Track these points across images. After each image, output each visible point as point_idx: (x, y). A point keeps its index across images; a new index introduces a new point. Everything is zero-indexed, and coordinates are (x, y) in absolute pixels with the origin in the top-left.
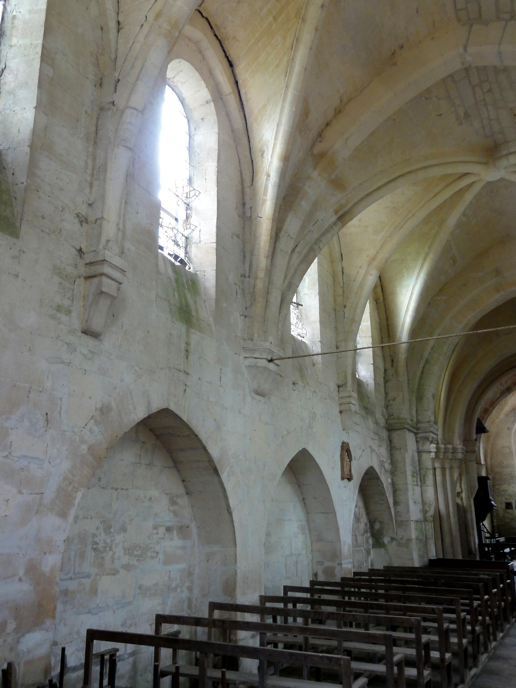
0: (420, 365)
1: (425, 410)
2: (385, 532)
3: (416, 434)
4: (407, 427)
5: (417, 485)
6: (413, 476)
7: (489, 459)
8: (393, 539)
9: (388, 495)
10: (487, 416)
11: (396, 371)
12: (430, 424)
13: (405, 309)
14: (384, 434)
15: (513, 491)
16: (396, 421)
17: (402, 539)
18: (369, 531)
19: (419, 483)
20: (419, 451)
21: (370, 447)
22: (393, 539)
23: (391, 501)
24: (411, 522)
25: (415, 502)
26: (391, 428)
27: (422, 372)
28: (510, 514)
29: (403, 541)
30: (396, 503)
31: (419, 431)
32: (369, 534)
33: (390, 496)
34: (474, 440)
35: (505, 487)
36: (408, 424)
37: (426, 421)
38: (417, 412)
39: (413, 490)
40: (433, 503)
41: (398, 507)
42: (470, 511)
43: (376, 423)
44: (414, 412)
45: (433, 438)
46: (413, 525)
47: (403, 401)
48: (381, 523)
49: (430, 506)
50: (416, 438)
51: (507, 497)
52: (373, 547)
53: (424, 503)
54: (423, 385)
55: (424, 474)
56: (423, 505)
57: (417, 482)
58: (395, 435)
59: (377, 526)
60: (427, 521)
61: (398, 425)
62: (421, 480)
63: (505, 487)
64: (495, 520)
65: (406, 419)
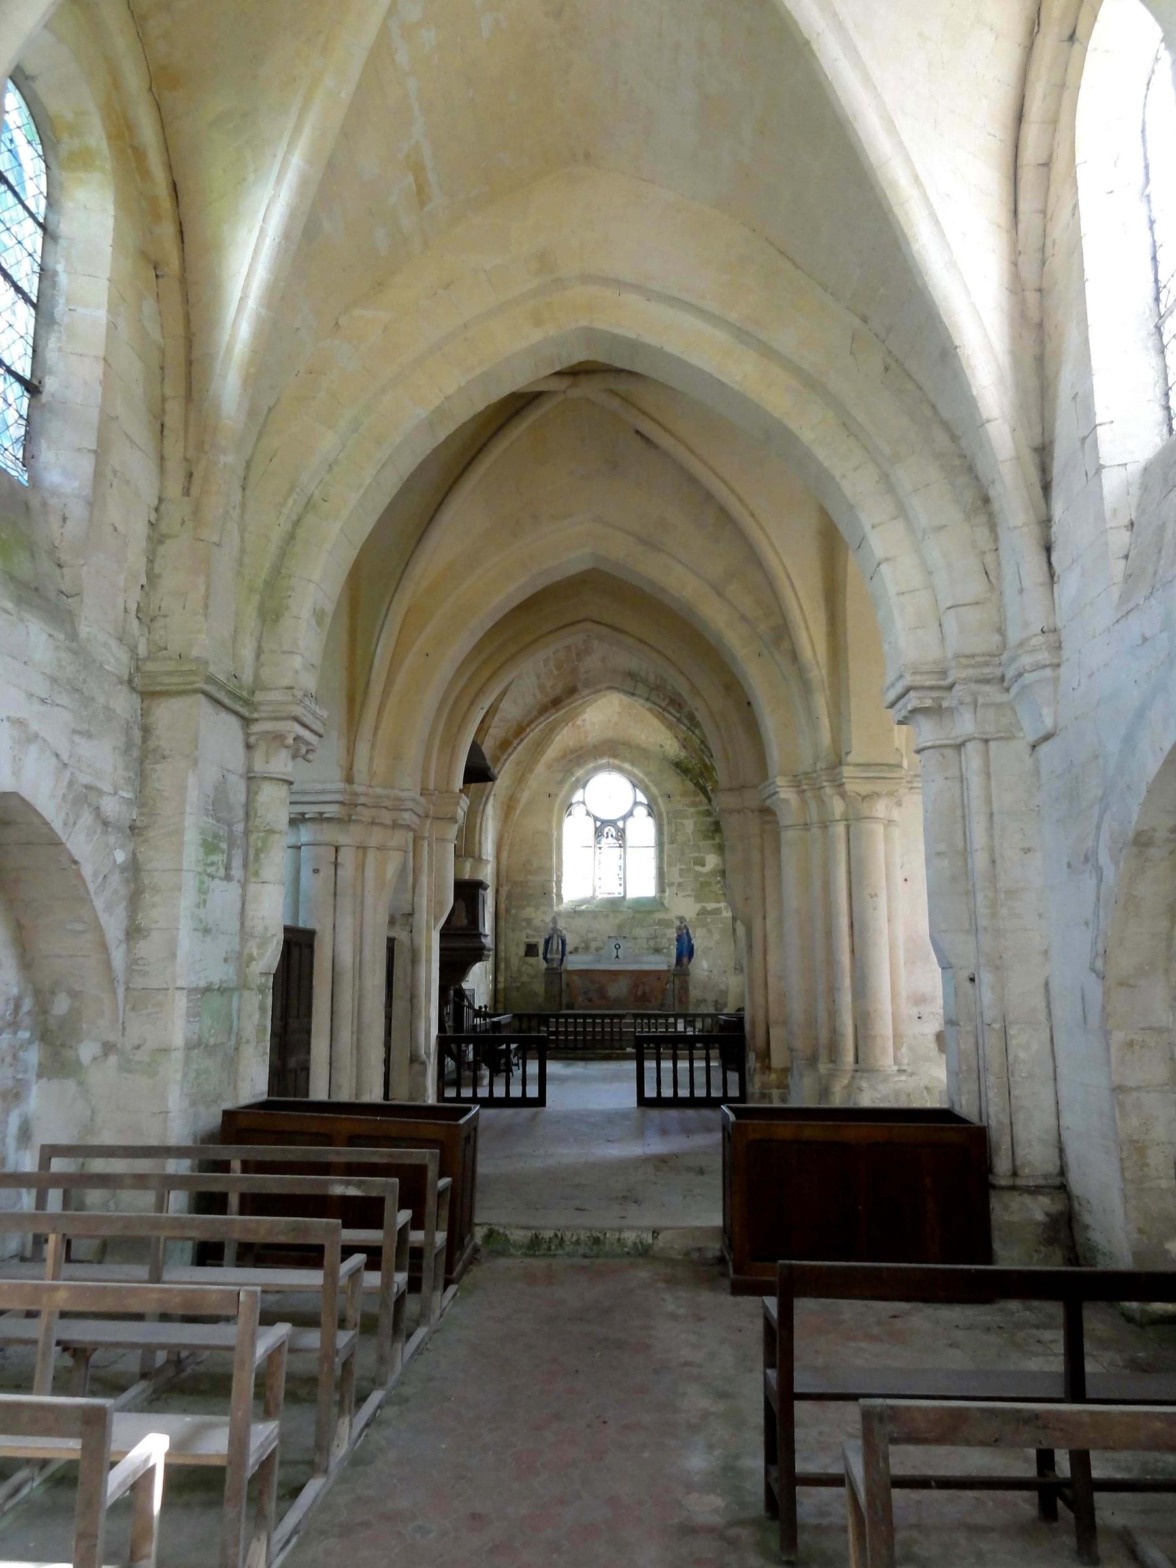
0: (285, 511)
1: (283, 652)
2: (85, 1026)
3: (246, 721)
4: (209, 688)
5: (228, 878)
6: (210, 847)
7: (504, 854)
8: (108, 1048)
9: (99, 903)
10: (505, 757)
11: (197, 510)
12: (293, 695)
13: (239, 295)
14: (124, 703)
15: (542, 921)
16: (171, 666)
17: (138, 1047)
18: (27, 1021)
19: (237, 872)
20: (252, 775)
21: (19, 723)
22: (108, 1048)
23: (113, 924)
24: (179, 992)
25: (207, 931)
26: (151, 689)
27: (291, 537)
28: (531, 965)
29: (142, 1056)
30: (134, 932)
31: (256, 715)
32: (25, 1035)
33: (109, 908)
34: (458, 791)
35: (529, 912)
36: (211, 679)
37: (286, 682)
38: (258, 656)
39: (202, 891)
40: (274, 935)
41: (142, 944)
42: (426, 961)
43: (77, 648)
44: (247, 653)
45: (297, 739)
46: (181, 1003)
47: (206, 606)
48: (74, 995)
49: (262, 945)
50: (248, 735)
51: (529, 931)
52: (39, 1076)
53: (244, 933)
54: (290, 577)
55: (260, 845)
56: (242, 938)
57: (228, 867)
58: (165, 713)
59: (61, 1005)
60: (249, 989)
61: (175, 680)
62: (245, 866)
63: (529, 912)
64: (501, 979)
65: (206, 663)
